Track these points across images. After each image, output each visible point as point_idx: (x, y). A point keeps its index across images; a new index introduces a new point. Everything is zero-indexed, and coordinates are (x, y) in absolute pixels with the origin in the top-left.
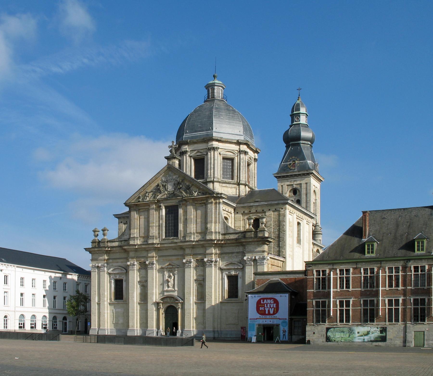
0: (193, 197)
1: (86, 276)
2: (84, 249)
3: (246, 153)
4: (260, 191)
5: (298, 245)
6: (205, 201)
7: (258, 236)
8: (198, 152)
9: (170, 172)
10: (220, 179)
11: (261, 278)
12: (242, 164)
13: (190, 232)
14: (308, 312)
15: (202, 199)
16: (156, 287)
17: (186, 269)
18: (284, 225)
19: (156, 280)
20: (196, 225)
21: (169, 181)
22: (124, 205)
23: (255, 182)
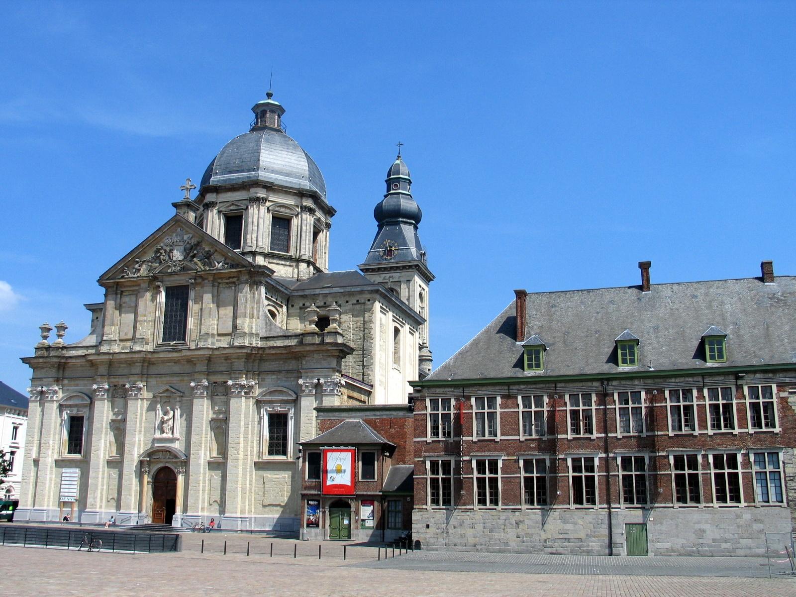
0: (215, 272)
1: (12, 407)
2: (21, 358)
3: (311, 211)
4: (332, 274)
5: (395, 366)
7: (325, 341)
8: (233, 204)
9: (179, 229)
10: (266, 250)
12: (304, 228)
14: (415, 483)
16: (140, 431)
18: (372, 329)
19: (141, 419)
20: (218, 320)
22: (98, 284)
23: (325, 261)
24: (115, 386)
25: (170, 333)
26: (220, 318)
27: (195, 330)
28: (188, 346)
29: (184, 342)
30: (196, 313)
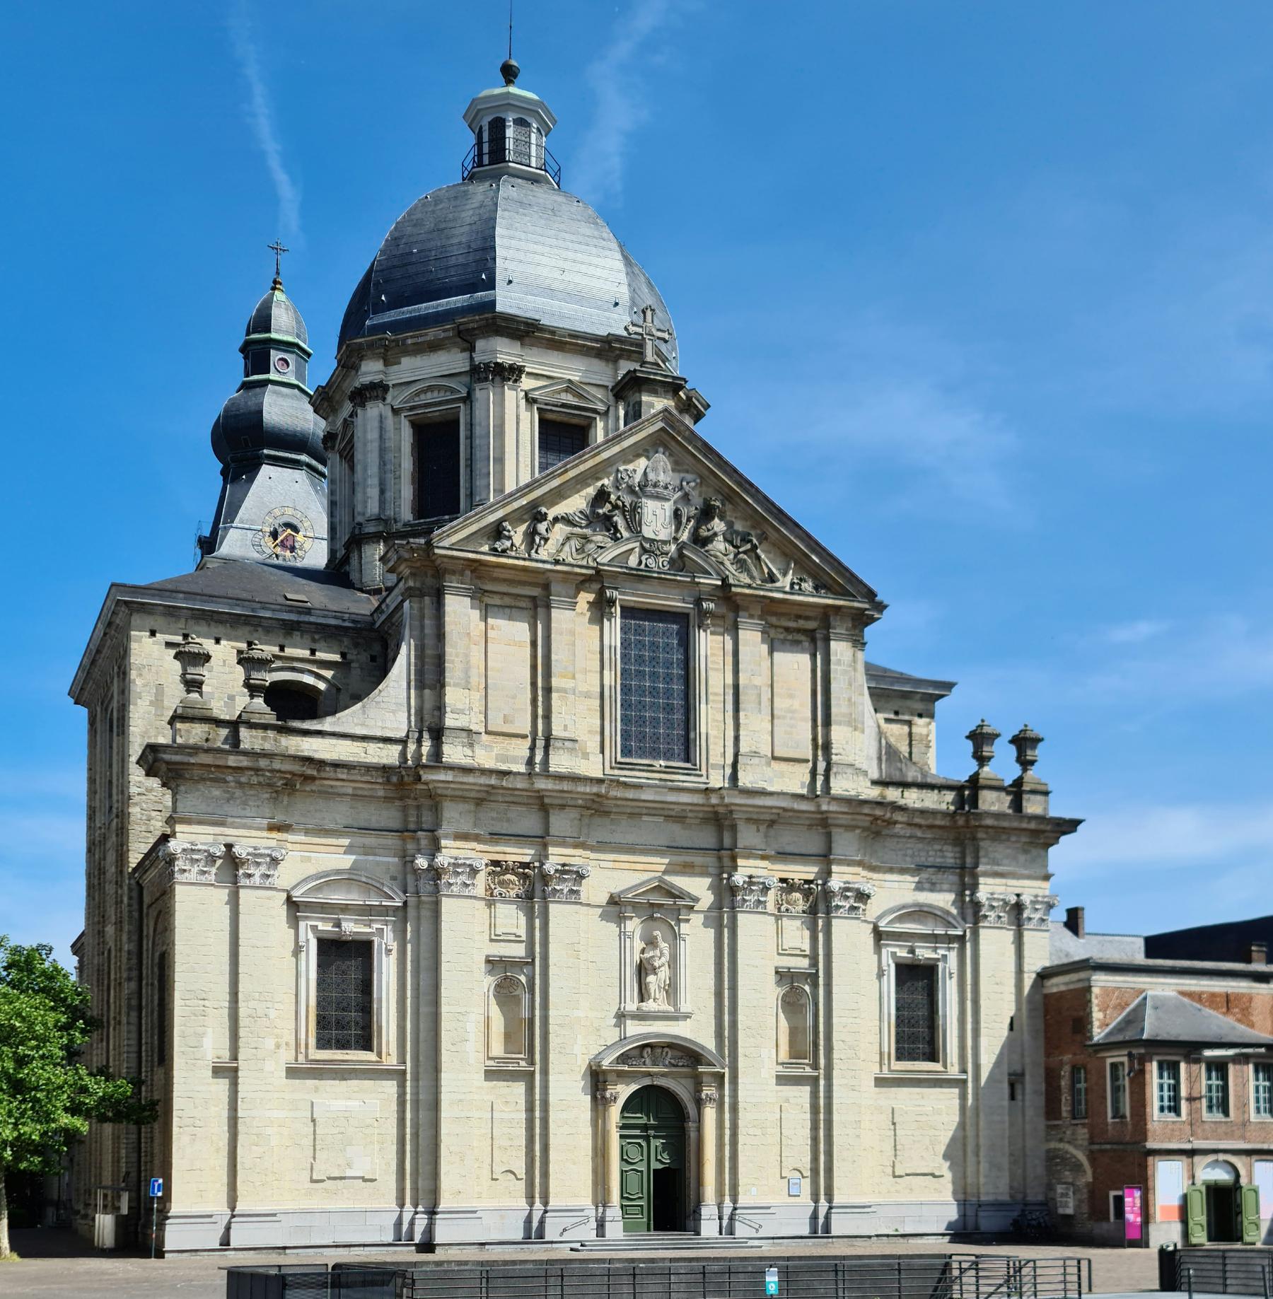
6: (811, 625)
8: (567, 390)
11: (1114, 985)
13: (754, 749)
15: (800, 611)
24: (496, 863)
25: (642, 737)
26: (779, 718)
27: (715, 737)
28: (703, 779)
29: (688, 765)
30: (716, 694)
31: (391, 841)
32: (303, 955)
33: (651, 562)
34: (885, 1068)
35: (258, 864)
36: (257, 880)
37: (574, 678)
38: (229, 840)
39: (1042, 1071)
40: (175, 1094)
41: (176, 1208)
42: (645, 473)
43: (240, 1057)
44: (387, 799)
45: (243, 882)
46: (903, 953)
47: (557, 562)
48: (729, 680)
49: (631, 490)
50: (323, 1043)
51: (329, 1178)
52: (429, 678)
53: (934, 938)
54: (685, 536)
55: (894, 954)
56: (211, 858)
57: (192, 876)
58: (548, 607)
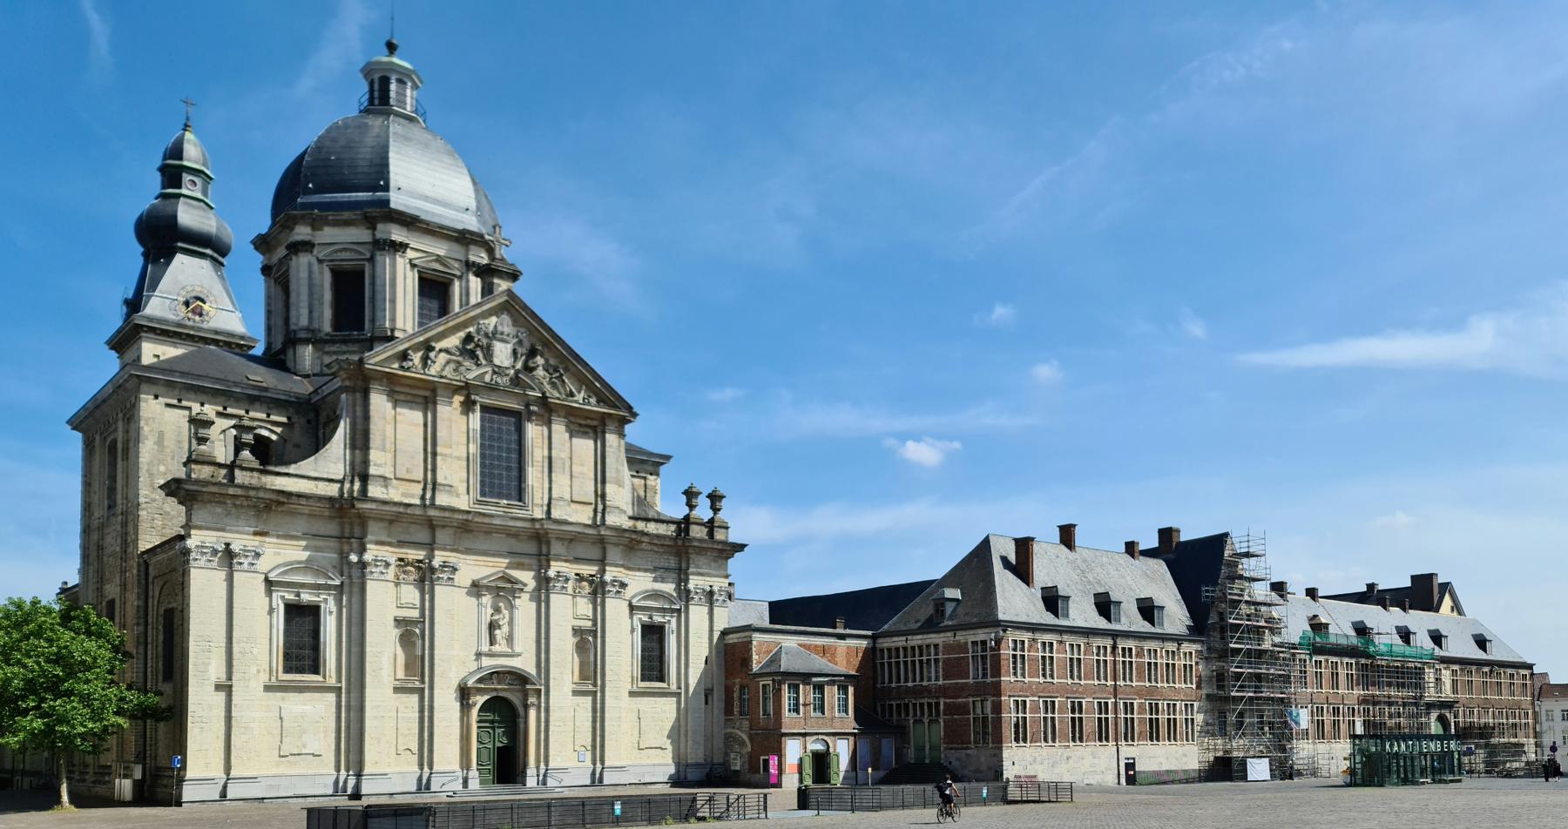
17: (553, 597)
21: (498, 336)
24: (401, 560)
25: (492, 486)
31: (333, 543)
32: (275, 614)
33: (499, 380)
34: (635, 686)
35: (247, 556)
36: (245, 566)
37: (451, 447)
38: (227, 541)
39: (723, 688)
40: (189, 702)
41: (190, 774)
42: (496, 326)
43: (234, 678)
44: (330, 517)
45: (236, 567)
46: (645, 619)
47: (442, 377)
48: (546, 453)
49: (486, 335)
50: (287, 670)
51: (291, 755)
52: (359, 443)
53: (663, 610)
54: (519, 365)
55: (640, 619)
56: (215, 552)
57: (202, 563)
58: (435, 403)
